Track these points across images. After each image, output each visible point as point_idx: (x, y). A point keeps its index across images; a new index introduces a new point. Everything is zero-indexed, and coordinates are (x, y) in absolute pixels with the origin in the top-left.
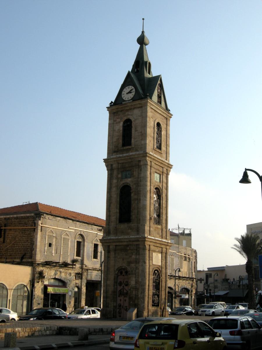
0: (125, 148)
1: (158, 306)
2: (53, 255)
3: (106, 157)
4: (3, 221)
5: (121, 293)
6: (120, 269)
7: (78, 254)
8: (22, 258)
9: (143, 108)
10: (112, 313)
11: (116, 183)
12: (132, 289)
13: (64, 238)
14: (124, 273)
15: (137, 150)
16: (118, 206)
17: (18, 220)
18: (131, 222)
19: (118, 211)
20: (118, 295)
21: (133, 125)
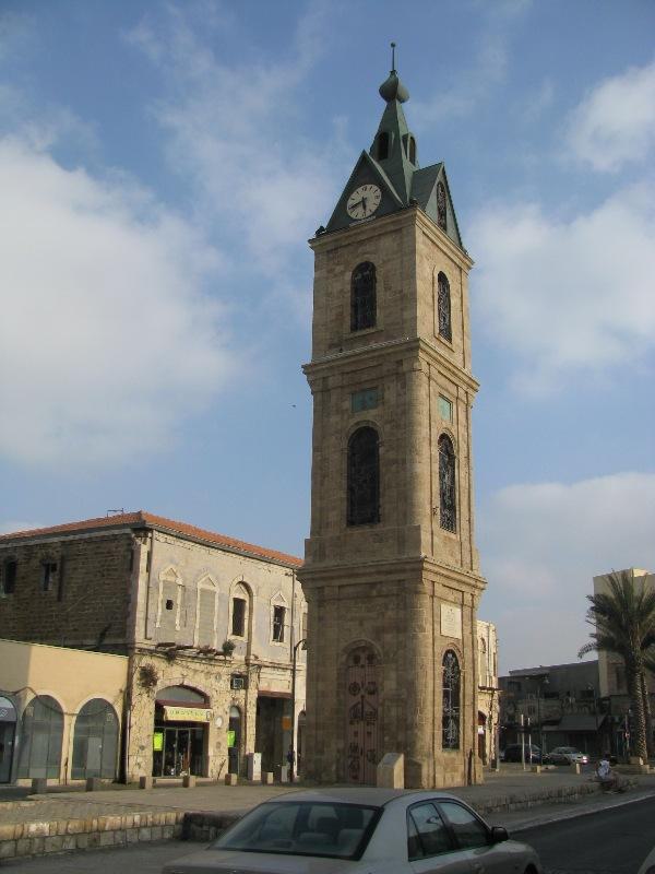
0: (358, 333)
1: (456, 747)
2: (178, 628)
4: (58, 549)
5: (357, 715)
6: (354, 650)
7: (238, 630)
8: (103, 635)
9: (403, 232)
10: (334, 768)
11: (337, 423)
12: (387, 703)
13: (203, 591)
14: (363, 661)
16: (344, 482)
17: (93, 546)
18: (379, 521)
19: (344, 496)
20: (348, 720)
21: (379, 277)
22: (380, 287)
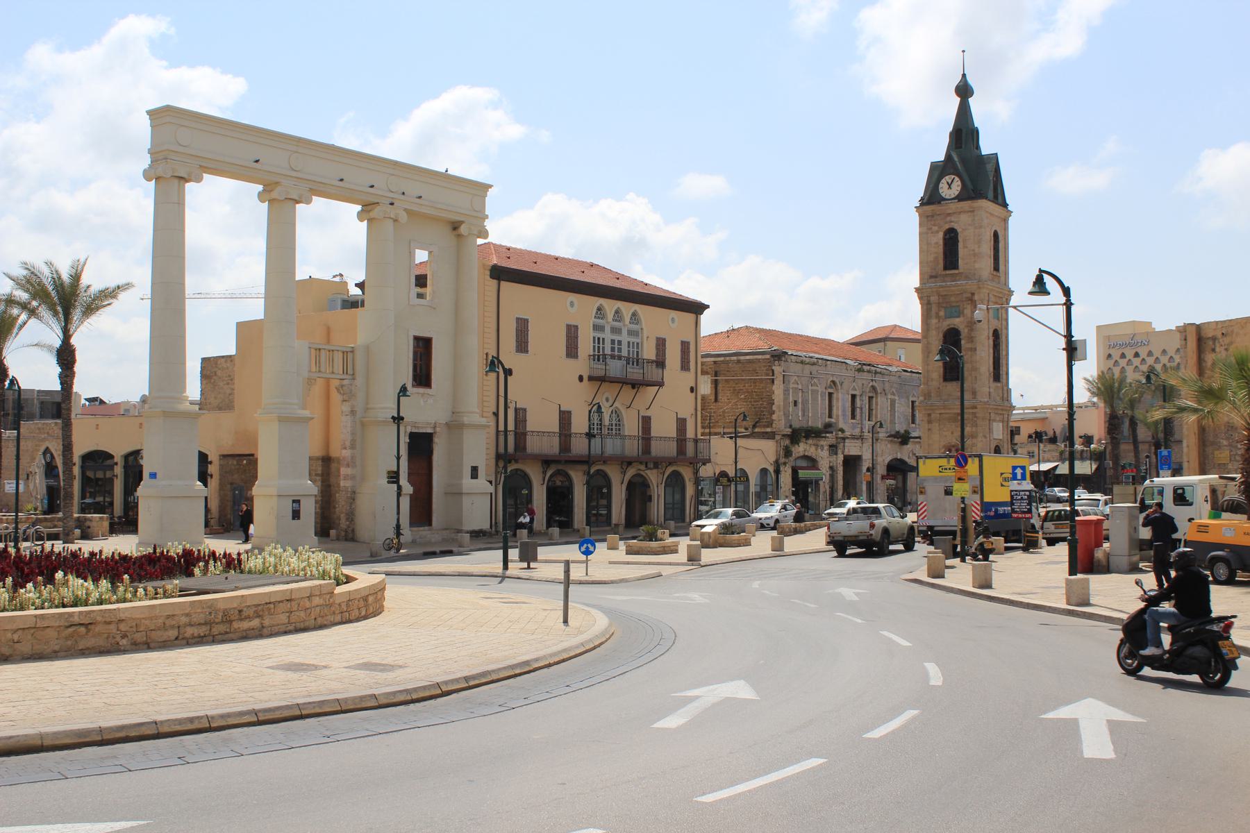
3: (918, 285)
15: (967, 278)
21: (960, 239)
22: (960, 245)
